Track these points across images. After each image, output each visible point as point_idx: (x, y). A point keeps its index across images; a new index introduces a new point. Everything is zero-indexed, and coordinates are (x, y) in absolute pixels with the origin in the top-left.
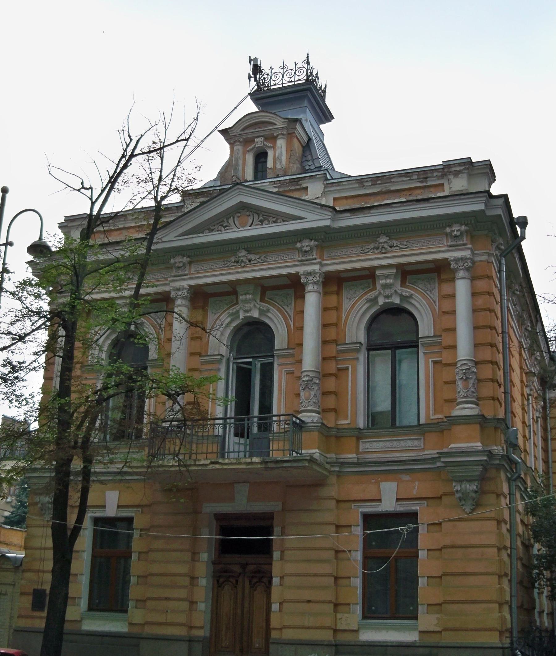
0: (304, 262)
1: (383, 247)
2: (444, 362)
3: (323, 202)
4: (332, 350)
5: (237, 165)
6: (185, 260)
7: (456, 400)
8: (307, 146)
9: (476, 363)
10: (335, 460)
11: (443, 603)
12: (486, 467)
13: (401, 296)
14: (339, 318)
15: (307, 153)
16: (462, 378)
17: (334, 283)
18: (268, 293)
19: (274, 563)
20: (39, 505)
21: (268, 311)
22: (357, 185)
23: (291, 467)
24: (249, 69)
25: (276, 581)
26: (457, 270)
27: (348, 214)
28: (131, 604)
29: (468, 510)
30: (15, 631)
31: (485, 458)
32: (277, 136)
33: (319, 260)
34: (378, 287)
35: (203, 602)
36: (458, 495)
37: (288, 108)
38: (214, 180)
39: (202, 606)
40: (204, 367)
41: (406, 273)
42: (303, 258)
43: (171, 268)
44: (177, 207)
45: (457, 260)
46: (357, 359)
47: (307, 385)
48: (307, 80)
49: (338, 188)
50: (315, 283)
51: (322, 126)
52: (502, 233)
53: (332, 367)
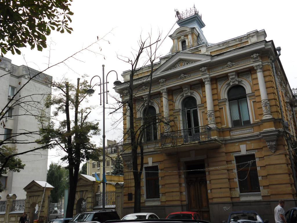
0: (203, 75)
1: (230, 66)
2: (257, 101)
3: (207, 54)
4: (217, 102)
5: (176, 46)
6: (164, 80)
7: (263, 114)
8: (198, 36)
9: (269, 100)
10: (223, 139)
11: (269, 185)
12: (278, 136)
13: (238, 81)
14: (218, 91)
15: (199, 39)
16: (264, 106)
17: (214, 81)
18: (192, 87)
19: (207, 176)
20: (127, 165)
21: (193, 93)
22: (217, 46)
23: (209, 143)
24: (175, 13)
25: (208, 182)
26: (257, 69)
27: (216, 57)
28: (160, 195)
29: (273, 152)
30: (123, 208)
31: (277, 133)
32: (188, 34)
33: (208, 73)
34: (230, 80)
35: (184, 192)
36: (268, 147)
37: (190, 25)
38: (169, 53)
39: (184, 193)
40: (175, 114)
41: (239, 74)
42: (203, 73)
43: (160, 83)
44: (159, 63)
45: (257, 66)
46: (225, 104)
47: (210, 115)
48: (195, 14)
49: (211, 48)
50: (208, 81)
51: (202, 29)
52: (272, 54)
53: (217, 108)
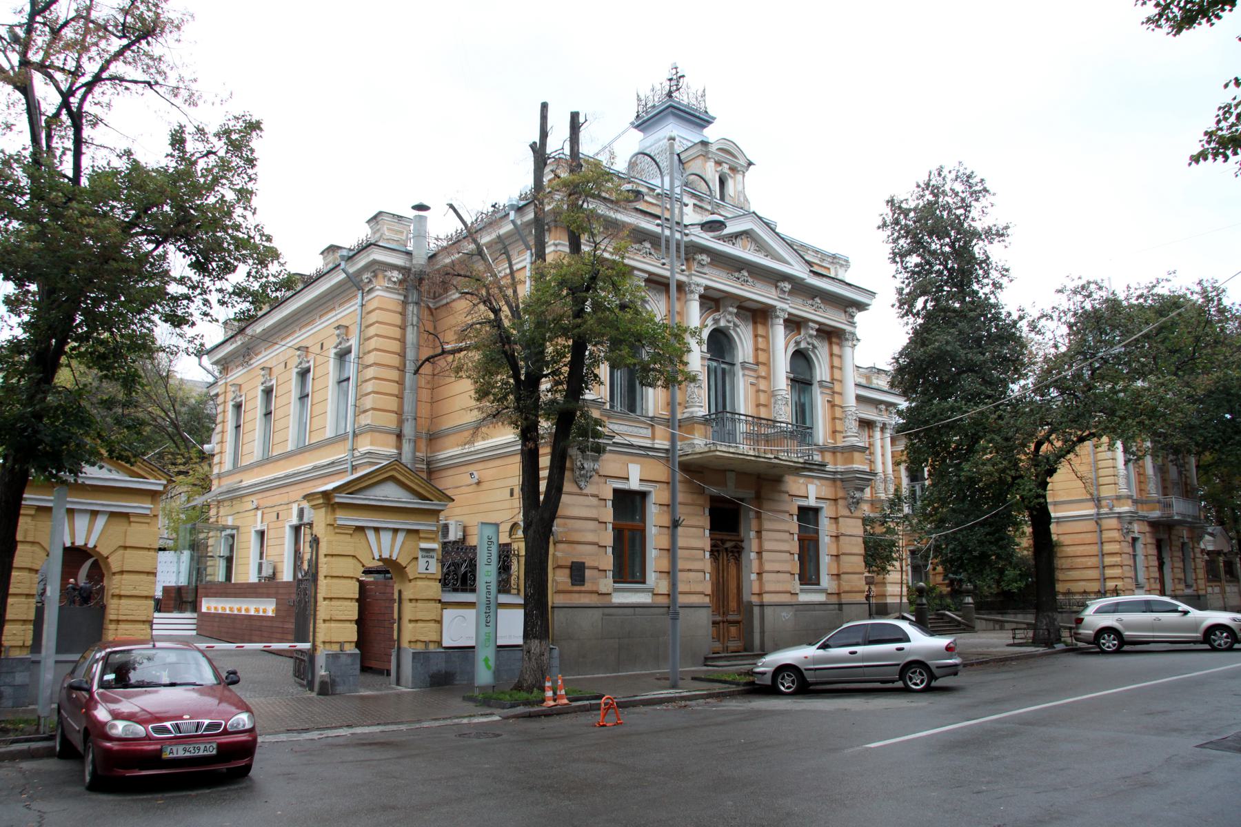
0: (782, 299)
